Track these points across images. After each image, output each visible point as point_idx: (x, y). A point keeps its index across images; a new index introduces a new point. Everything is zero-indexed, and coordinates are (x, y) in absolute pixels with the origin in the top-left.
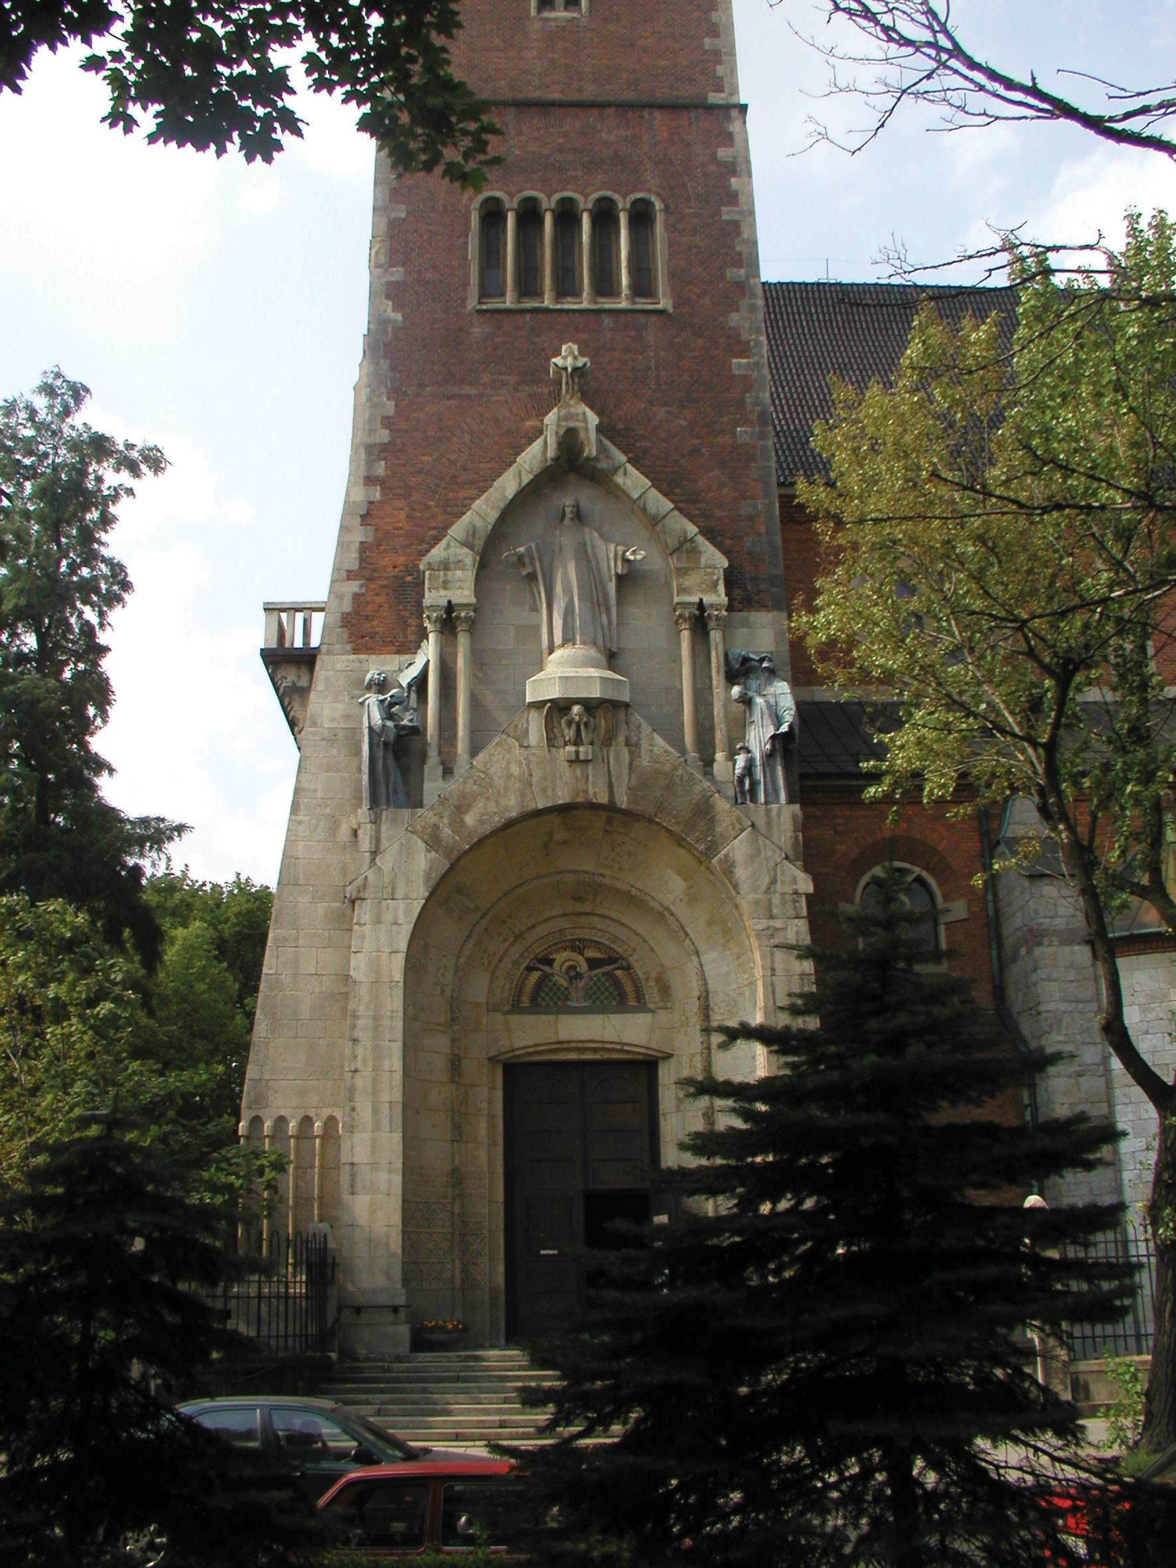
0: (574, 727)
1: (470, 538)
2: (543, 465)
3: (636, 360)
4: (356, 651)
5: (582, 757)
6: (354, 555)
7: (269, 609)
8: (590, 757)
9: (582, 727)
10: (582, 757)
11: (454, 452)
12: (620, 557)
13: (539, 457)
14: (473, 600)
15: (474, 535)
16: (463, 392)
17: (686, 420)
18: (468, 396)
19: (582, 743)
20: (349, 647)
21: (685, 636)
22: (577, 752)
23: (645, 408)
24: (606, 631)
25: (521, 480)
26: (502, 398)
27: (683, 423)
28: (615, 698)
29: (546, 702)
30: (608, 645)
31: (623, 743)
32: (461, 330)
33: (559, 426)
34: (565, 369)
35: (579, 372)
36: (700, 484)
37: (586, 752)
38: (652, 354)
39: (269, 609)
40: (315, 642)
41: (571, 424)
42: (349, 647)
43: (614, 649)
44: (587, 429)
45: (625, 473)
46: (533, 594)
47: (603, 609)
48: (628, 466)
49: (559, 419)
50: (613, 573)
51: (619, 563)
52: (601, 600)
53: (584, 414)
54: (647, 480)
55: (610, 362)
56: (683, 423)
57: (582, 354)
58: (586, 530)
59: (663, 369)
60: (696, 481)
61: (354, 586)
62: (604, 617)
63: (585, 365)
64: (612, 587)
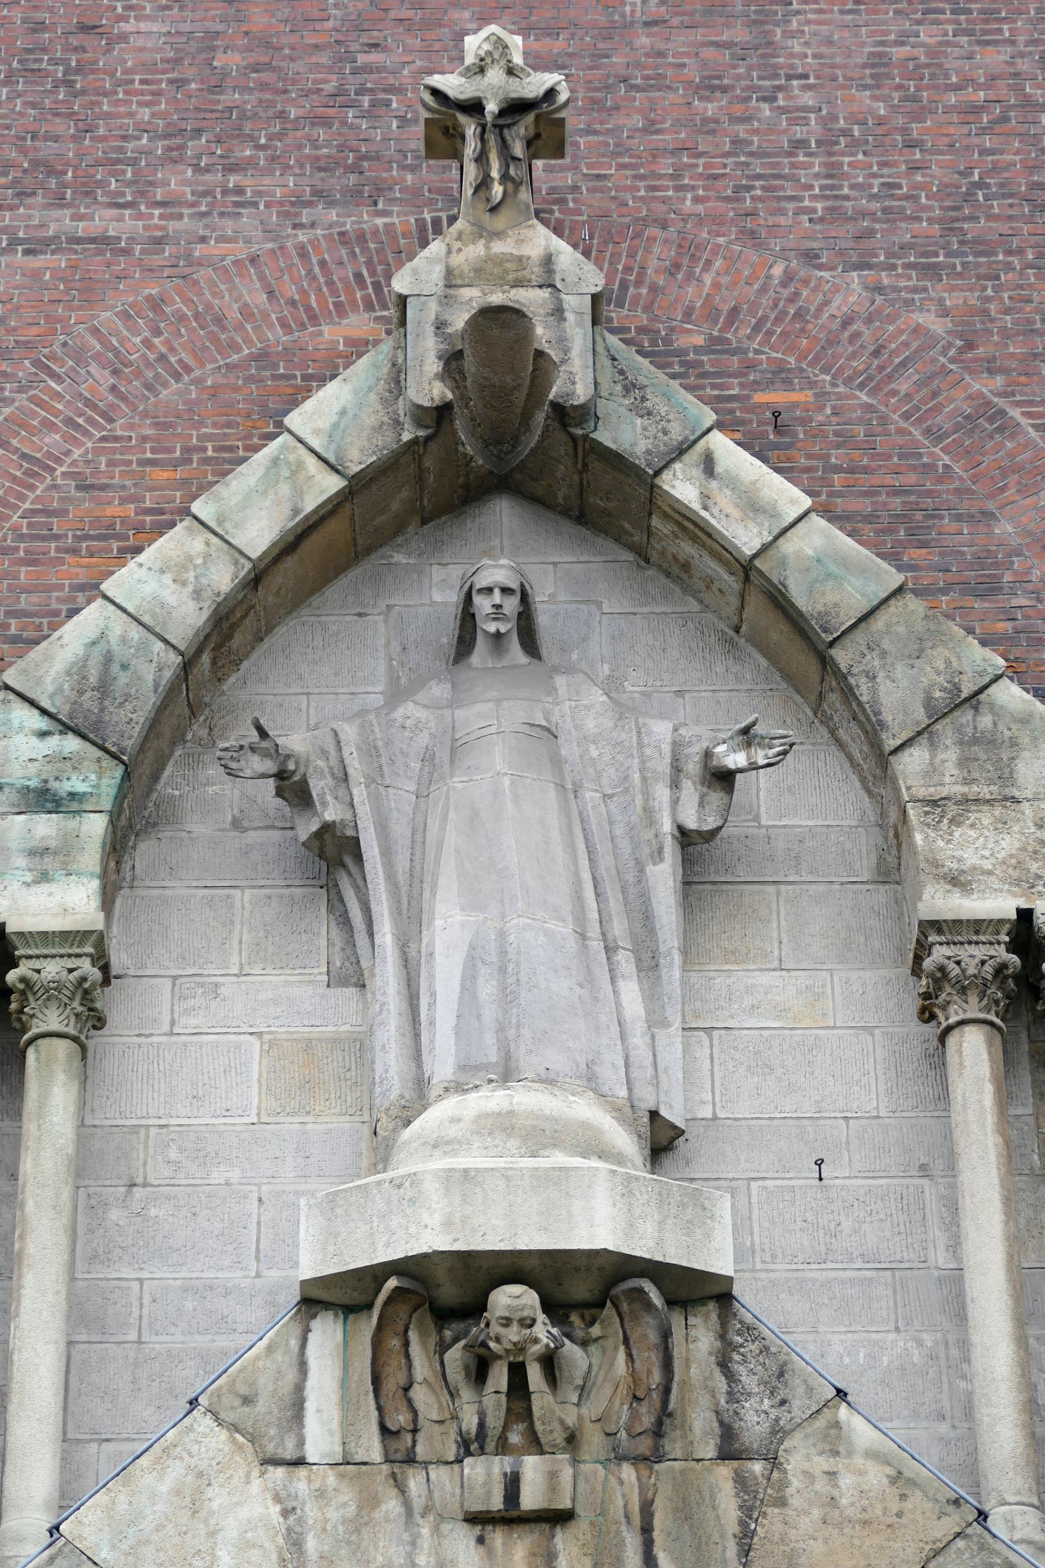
0: (499, 1377)
1: (89, 701)
2: (386, 443)
3: (747, 120)
5: (530, 1499)
8: (566, 1504)
9: (535, 1375)
10: (530, 1499)
11: (51, 427)
12: (693, 766)
13: (372, 415)
14: (100, 926)
15: (104, 688)
16: (81, 228)
17: (944, 313)
18: (102, 241)
19: (535, 1444)
22: (513, 1485)
23: (788, 278)
24: (638, 1041)
25: (299, 493)
26: (240, 249)
27: (938, 326)
28: (674, 1254)
29: (378, 1273)
30: (647, 1099)
31: (708, 1450)
32: (86, 28)
33: (447, 300)
34: (474, 107)
36: (1005, 528)
37: (553, 1476)
38: (808, 99)
41: (497, 298)
43: (672, 1114)
44: (558, 312)
45: (708, 464)
46: (345, 922)
47: (625, 961)
48: (720, 443)
49: (451, 280)
50: (667, 827)
53: (548, 261)
54: (796, 492)
55: (651, 127)
56: (938, 326)
57: (538, 63)
58: (560, 681)
59: (855, 144)
60: (988, 515)
62: (631, 992)
63: (551, 93)
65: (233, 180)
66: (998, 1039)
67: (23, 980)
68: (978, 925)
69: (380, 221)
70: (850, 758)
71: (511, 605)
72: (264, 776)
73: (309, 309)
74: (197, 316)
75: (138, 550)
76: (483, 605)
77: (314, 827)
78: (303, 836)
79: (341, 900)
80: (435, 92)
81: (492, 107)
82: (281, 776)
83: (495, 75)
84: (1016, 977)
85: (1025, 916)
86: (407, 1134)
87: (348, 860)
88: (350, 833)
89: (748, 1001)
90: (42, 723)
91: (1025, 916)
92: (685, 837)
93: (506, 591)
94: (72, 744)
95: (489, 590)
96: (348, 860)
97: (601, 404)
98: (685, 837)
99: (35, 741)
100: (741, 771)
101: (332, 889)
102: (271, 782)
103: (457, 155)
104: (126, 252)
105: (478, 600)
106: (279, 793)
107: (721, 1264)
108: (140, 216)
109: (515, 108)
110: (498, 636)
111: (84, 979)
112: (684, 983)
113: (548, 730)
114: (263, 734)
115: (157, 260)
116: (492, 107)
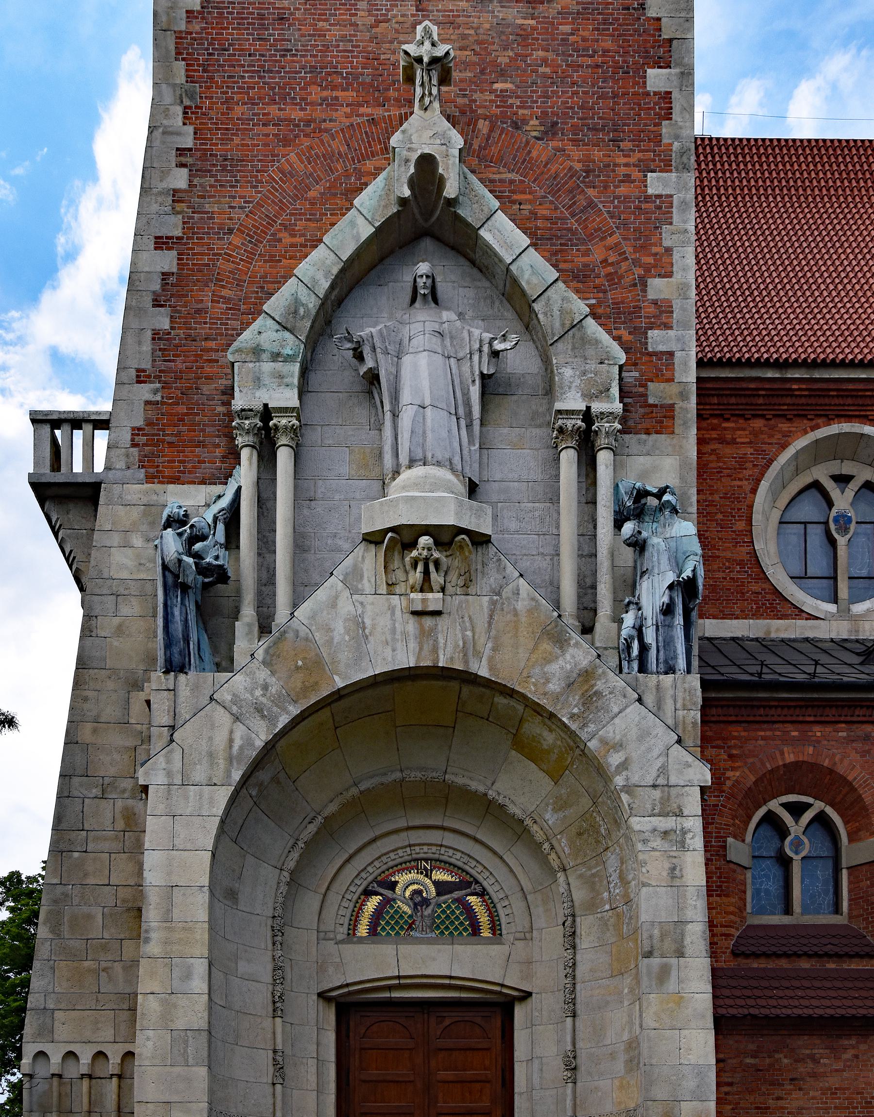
4: (150, 479)
6: (147, 346)
7: (38, 419)
20: (141, 474)
21: (569, 459)
34: (419, 60)
35: (438, 66)
39: (38, 419)
40: (99, 466)
42: (141, 474)
50: (477, 373)
51: (485, 358)
52: (461, 411)
57: (444, 41)
61: (146, 392)
63: (447, 53)
64: (475, 391)
65: (334, 94)
66: (576, 454)
67: (275, 425)
68: (572, 412)
69: (386, 114)
70: (537, 348)
71: (430, 281)
72: (349, 349)
73: (362, 154)
74: (324, 155)
75: (306, 257)
76: (421, 282)
77: (365, 370)
78: (361, 374)
79: (374, 398)
80: (406, 53)
81: (426, 59)
82: (355, 349)
83: (427, 44)
84: (583, 431)
85: (588, 408)
86: (394, 483)
87: (375, 382)
88: (376, 372)
89: (500, 439)
90: (278, 327)
91: (588, 408)
92: (483, 376)
93: (427, 277)
94: (287, 335)
95: (422, 276)
96: (375, 382)
97: (461, 198)
98: (483, 376)
99: (275, 333)
100: (502, 351)
101: (370, 393)
102: (351, 352)
103: (414, 83)
104: (298, 126)
105: (418, 280)
106: (354, 357)
107: (488, 531)
108: (302, 109)
109: (434, 60)
110: (424, 295)
111: (293, 425)
112: (481, 432)
113: (439, 333)
114: (349, 333)
115: (308, 130)
116: (426, 59)
